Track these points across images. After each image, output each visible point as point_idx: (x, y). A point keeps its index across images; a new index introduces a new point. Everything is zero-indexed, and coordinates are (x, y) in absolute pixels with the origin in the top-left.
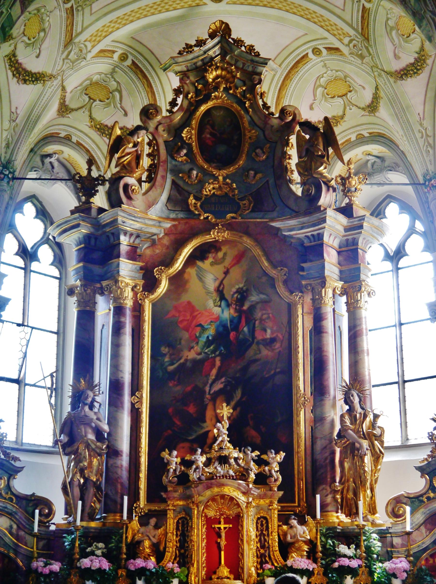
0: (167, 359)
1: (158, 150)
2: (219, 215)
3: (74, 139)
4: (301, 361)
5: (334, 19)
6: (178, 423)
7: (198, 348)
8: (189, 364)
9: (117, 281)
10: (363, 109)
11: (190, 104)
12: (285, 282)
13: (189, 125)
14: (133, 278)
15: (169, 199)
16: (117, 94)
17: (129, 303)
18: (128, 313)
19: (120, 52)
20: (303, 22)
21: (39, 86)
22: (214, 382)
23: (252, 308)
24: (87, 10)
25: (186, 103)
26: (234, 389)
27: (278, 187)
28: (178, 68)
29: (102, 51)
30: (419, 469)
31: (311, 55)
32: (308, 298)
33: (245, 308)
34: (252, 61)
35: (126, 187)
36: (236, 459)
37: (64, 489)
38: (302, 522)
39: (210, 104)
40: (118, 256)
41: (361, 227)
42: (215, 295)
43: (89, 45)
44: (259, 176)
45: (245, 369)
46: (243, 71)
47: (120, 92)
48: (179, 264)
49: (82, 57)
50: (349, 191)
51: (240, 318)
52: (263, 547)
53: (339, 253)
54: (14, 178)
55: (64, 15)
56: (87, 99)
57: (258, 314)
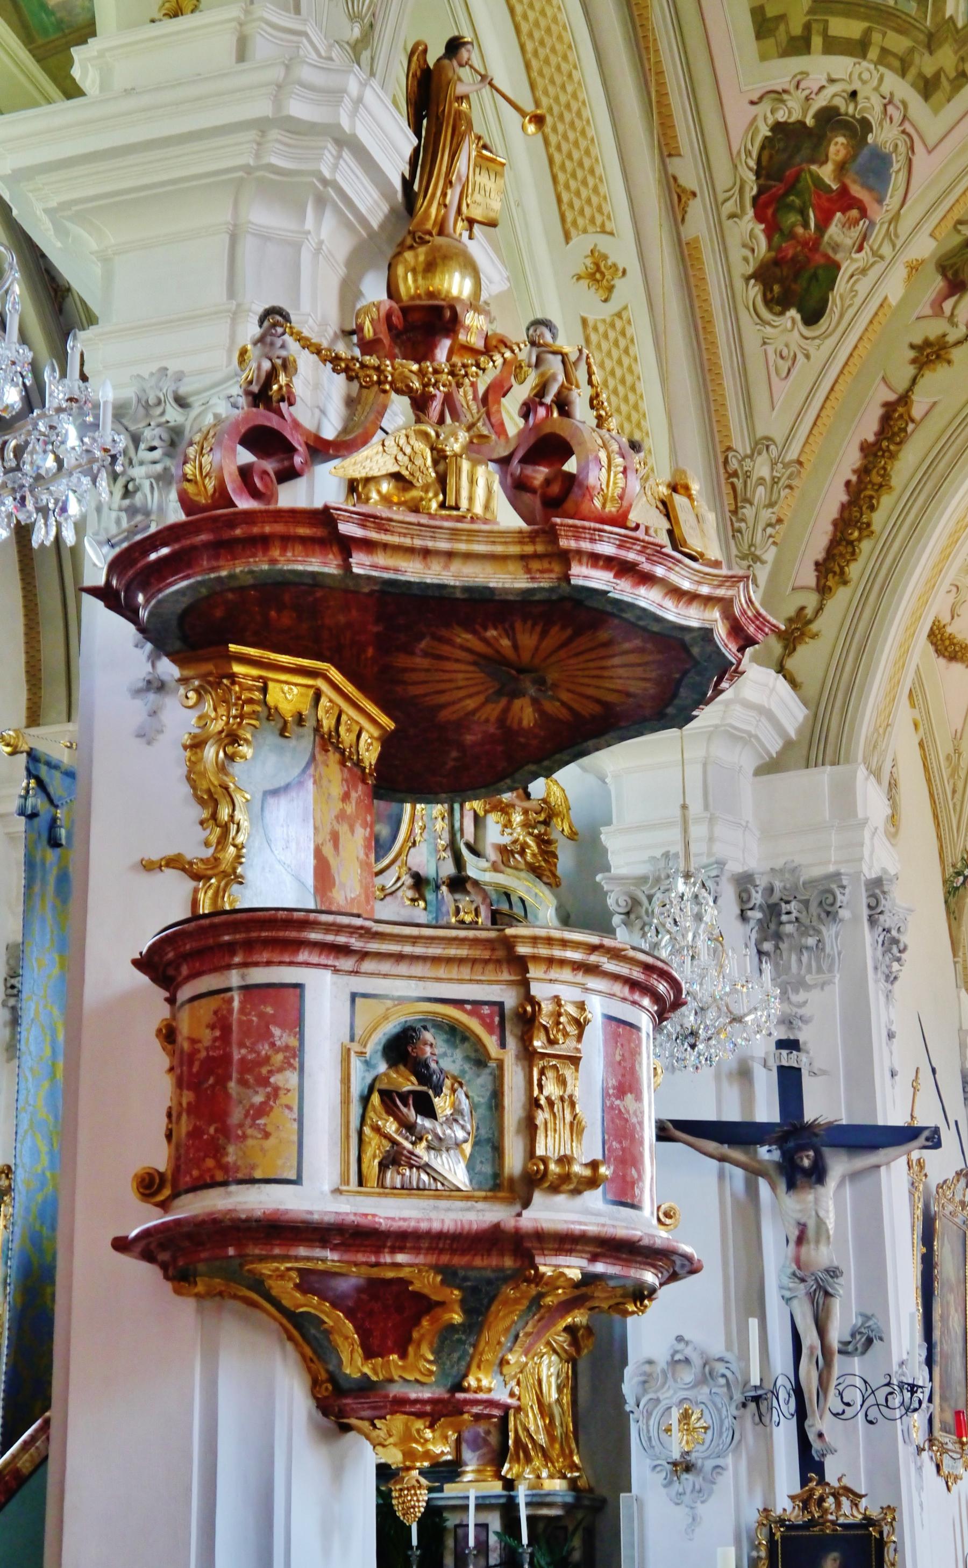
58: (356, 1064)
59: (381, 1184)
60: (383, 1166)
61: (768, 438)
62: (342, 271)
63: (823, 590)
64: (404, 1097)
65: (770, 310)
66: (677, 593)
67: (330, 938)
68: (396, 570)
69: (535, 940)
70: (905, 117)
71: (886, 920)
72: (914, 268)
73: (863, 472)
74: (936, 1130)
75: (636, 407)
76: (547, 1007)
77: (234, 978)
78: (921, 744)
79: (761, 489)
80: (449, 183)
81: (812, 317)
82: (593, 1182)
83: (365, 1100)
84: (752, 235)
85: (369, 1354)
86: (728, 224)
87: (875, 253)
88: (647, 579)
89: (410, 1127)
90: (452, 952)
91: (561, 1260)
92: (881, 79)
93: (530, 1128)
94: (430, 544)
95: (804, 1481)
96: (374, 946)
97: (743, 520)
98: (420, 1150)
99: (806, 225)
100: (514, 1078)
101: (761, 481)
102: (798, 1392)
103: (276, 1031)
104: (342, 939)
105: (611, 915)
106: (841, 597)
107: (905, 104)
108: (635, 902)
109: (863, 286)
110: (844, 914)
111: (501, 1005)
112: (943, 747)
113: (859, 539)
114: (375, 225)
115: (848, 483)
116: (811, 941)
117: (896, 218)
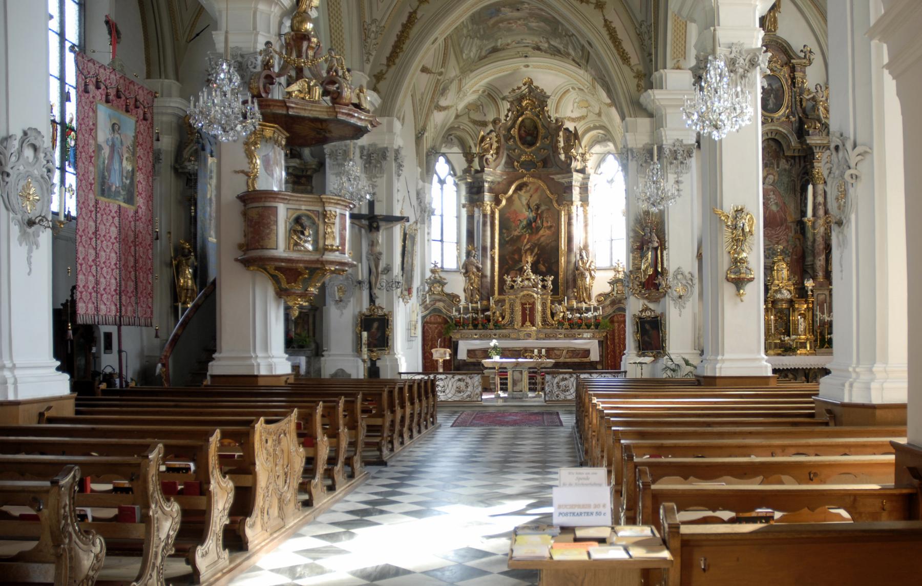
3: (461, 127)
4: (563, 236)
5: (580, 78)
7: (518, 230)
12: (557, 201)
13: (514, 127)
14: (490, 201)
15: (506, 163)
17: (489, 212)
18: (488, 217)
21: (446, 112)
23: (542, 212)
24: (467, 78)
26: (534, 248)
27: (554, 157)
32: (566, 208)
35: (487, 159)
37: (465, 291)
38: (560, 304)
39: (524, 116)
45: (539, 239)
46: (539, 100)
48: (511, 192)
49: (465, 95)
53: (580, 188)
57: (545, 215)
64: (298, 231)
66: (360, 119)
69: (327, 198)
71: (399, 161)
77: (261, 204)
82: (338, 250)
83: (290, 231)
85: (288, 283)
88: (354, 116)
89: (299, 238)
93: (325, 239)
95: (370, 305)
98: (302, 243)
102: (370, 283)
105: (325, 154)
106: (393, 68)
108: (333, 152)
112: (418, 97)
116: (379, 165)
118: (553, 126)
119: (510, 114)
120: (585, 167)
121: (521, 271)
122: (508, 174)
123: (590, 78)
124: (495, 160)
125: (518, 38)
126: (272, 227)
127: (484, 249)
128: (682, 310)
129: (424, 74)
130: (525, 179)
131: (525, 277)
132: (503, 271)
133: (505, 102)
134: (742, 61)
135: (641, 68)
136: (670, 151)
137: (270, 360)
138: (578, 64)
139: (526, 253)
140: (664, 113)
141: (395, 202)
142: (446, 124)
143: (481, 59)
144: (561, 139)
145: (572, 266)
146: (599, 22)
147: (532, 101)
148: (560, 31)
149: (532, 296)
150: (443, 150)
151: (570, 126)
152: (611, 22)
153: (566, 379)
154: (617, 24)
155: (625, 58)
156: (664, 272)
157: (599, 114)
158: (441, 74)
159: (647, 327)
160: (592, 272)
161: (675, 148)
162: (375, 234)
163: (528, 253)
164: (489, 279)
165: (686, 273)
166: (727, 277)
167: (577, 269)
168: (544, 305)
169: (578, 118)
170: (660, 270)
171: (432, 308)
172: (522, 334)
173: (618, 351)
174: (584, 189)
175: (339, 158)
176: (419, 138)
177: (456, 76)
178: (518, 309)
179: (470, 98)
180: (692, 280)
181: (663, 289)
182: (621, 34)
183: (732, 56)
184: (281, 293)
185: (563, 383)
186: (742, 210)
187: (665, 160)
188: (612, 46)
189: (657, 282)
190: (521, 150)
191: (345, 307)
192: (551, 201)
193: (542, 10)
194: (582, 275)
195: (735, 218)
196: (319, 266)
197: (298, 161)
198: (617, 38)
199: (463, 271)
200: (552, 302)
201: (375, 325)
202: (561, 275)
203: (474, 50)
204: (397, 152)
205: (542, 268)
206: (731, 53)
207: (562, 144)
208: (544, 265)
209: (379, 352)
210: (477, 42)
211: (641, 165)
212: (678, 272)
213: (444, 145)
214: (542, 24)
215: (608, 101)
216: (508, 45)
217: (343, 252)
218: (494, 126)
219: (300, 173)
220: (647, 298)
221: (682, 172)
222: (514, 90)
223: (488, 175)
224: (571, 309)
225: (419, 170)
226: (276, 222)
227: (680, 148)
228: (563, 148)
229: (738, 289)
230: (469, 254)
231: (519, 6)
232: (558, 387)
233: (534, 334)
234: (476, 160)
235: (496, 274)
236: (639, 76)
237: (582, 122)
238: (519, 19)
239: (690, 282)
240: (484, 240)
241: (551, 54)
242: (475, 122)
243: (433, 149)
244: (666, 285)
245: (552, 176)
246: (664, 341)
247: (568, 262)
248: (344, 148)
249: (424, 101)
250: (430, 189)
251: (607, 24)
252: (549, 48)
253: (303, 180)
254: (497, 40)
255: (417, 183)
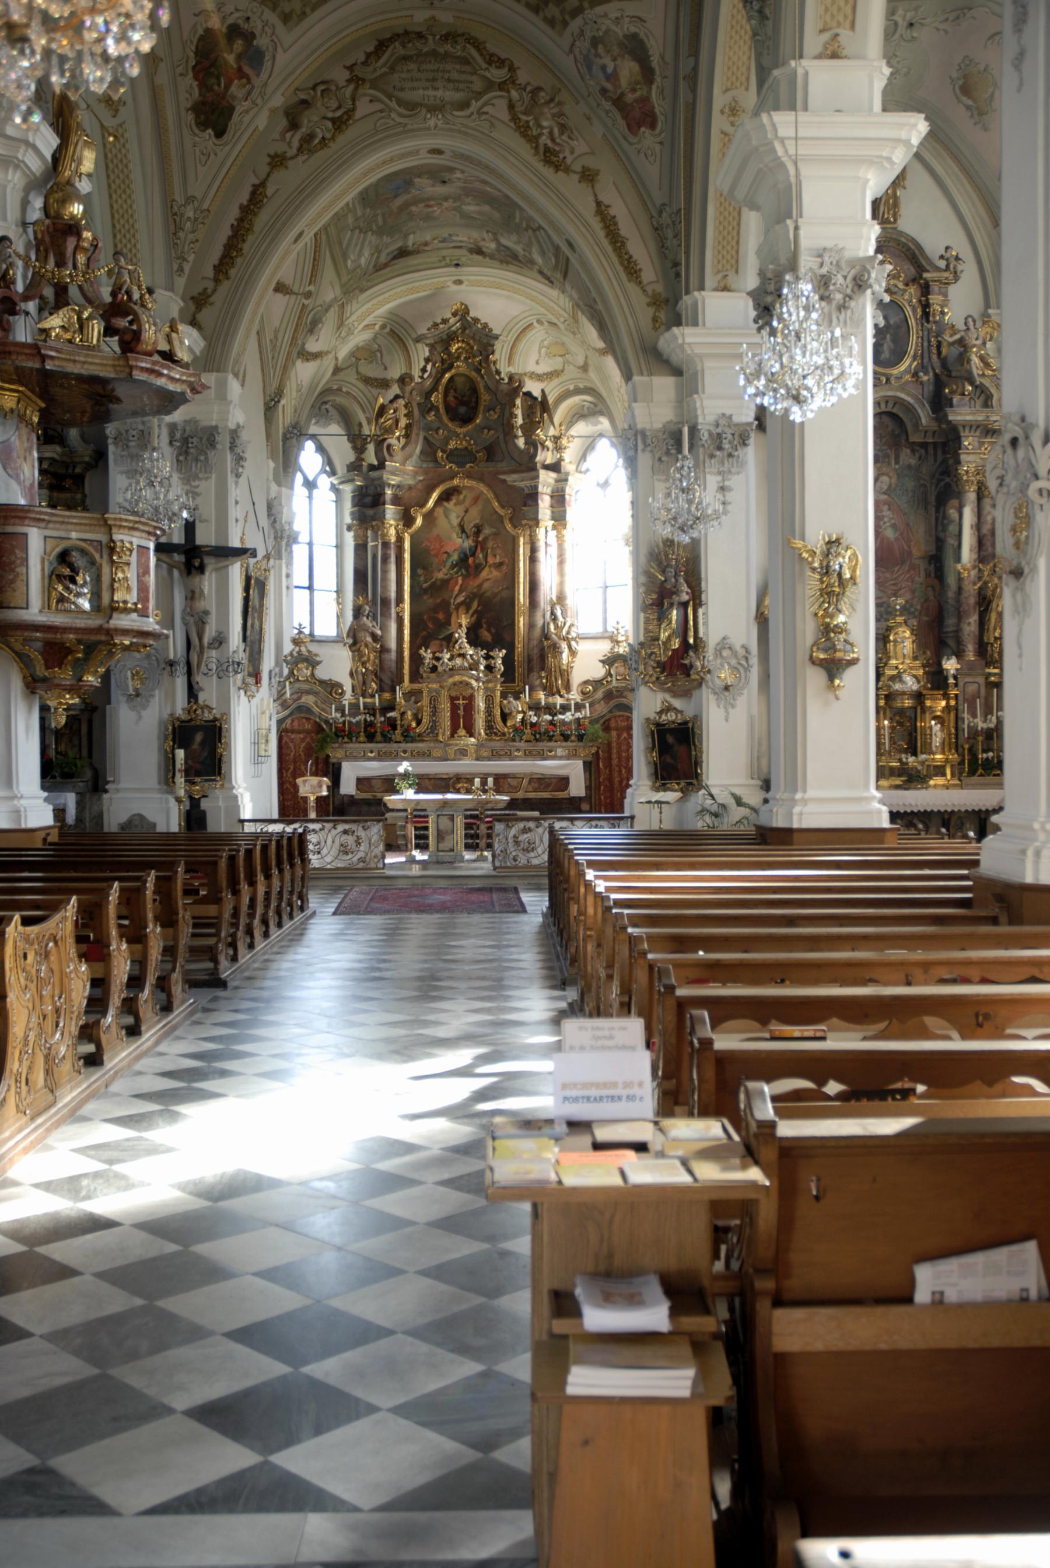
0: (422, 579)
1: (412, 412)
2: (461, 465)
3: (344, 389)
4: (522, 580)
5: (552, 304)
6: (431, 626)
7: (444, 570)
8: (438, 583)
9: (383, 523)
10: (579, 368)
11: (438, 372)
12: (511, 520)
13: (437, 390)
14: (395, 520)
15: (422, 452)
16: (378, 354)
17: (393, 539)
18: (392, 546)
19: (380, 323)
20: (528, 301)
21: (318, 361)
22: (457, 595)
23: (486, 539)
24: (354, 302)
25: (434, 371)
27: (506, 442)
28: (428, 342)
29: (367, 326)
30: (602, 661)
31: (535, 324)
32: (528, 532)
33: (480, 539)
34: (487, 335)
35: (389, 446)
36: (471, 656)
37: (351, 675)
38: (517, 698)
39: (453, 371)
40: (384, 504)
41: (566, 480)
42: (458, 529)
43: (356, 324)
44: (492, 432)
45: (480, 586)
47: (381, 352)
48: (431, 503)
49: (350, 332)
50: (560, 448)
51: (476, 547)
52: (490, 715)
53: (552, 497)
54: (301, 435)
55: (337, 309)
56: (354, 360)
57: (490, 544)
58: (46, 563)
59: (57, 609)
60: (58, 602)
61: (194, 197)
62: (22, 194)
63: (217, 281)
64: (65, 577)
65: (198, 128)
66: (172, 379)
67: (38, 516)
68: (62, 367)
69: (115, 519)
70: (273, 33)
71: (238, 450)
72: (273, 111)
73: (241, 220)
74: (255, 550)
75: (128, 176)
76: (118, 544)
78: (258, 333)
79: (188, 224)
80: (73, 160)
81: (220, 134)
82: (136, 610)
83: (50, 577)
84: (191, 86)
85: (47, 668)
86: (179, 79)
87: (253, 103)
88: (160, 374)
89: (67, 588)
90: (83, 521)
91: (122, 638)
92: (262, 13)
93: (113, 590)
94: (77, 358)
95: (189, 702)
96: (54, 519)
97: (179, 239)
98: (71, 597)
99: (219, 85)
100: (106, 570)
101: (189, 219)
102: (189, 664)
103: (17, 551)
104: (42, 517)
106: (225, 286)
107: (273, 26)
109: (246, 119)
110: (219, 446)
111: (101, 542)
112: (269, 336)
113: (236, 256)
114: (38, 175)
115: (232, 225)
116: (202, 458)
117: (265, 85)
118: (504, 388)
119: (429, 367)
120: (561, 460)
121: (449, 641)
122: (426, 472)
123: (569, 305)
124: (403, 448)
125: (444, 233)
126: (18, 570)
127: (385, 602)
128: (730, 710)
129: (279, 296)
130: (456, 482)
131: (455, 652)
132: (419, 641)
133: (419, 346)
134: (840, 280)
135: (659, 288)
136: (711, 434)
137: (16, 802)
138: (548, 279)
139: (457, 608)
140: (699, 368)
141: (231, 523)
142: (318, 384)
143: (379, 268)
144: (519, 412)
145: (537, 632)
146: (588, 209)
147: (468, 344)
148: (517, 220)
149: (468, 684)
150: (313, 429)
151: (534, 388)
152: (608, 206)
153: (530, 830)
154: (618, 209)
155: (632, 271)
156: (698, 646)
157: (585, 368)
158: (308, 295)
159: (670, 739)
160: (573, 643)
161: (719, 430)
162: (197, 579)
163: (462, 610)
164: (393, 655)
165: (738, 647)
166: (811, 657)
167: (546, 636)
168: (489, 699)
169: (547, 374)
170: (691, 641)
171: (294, 706)
172: (451, 751)
173: (617, 779)
174: (559, 499)
175: (132, 444)
176: (270, 408)
177: (335, 299)
178: (445, 706)
179: (360, 337)
180: (747, 659)
181: (698, 673)
182: (626, 228)
183: (824, 271)
184: (33, 684)
185: (525, 836)
186: (838, 541)
187: (701, 450)
188: (609, 249)
189: (686, 662)
190: (449, 431)
191: (144, 707)
192: (501, 519)
193: (486, 183)
194: (555, 648)
195: (827, 554)
196: (103, 638)
197: (58, 449)
198: (618, 234)
199: (350, 641)
200: (504, 695)
201: (199, 737)
202: (519, 647)
203: (366, 253)
204: (234, 434)
205: (486, 635)
206: (822, 265)
207: (520, 421)
208: (489, 630)
209: (206, 784)
210: (371, 237)
211: (660, 459)
212: (724, 644)
213: (314, 421)
214: (486, 208)
215: (601, 344)
216: (426, 244)
217: (144, 614)
218: (401, 389)
219: (62, 471)
220: (669, 690)
221: (730, 472)
222: (436, 325)
223: (393, 473)
224: (536, 707)
225: (272, 465)
226: (26, 560)
227: (727, 430)
228: (521, 426)
229: (831, 678)
230: (358, 612)
231: (447, 176)
232: (517, 843)
233: (472, 750)
234: (371, 448)
235: (406, 646)
236: (656, 302)
237: (556, 381)
238: (446, 199)
239: (744, 662)
240: (385, 588)
241: (501, 262)
242: (368, 381)
243: (294, 427)
244: (703, 667)
245: (502, 477)
246: (698, 763)
247: (531, 626)
248: (141, 427)
249: (279, 344)
250: (290, 498)
251: (601, 210)
252: (498, 251)
253: (68, 483)
254: (406, 236)
255: (268, 489)
